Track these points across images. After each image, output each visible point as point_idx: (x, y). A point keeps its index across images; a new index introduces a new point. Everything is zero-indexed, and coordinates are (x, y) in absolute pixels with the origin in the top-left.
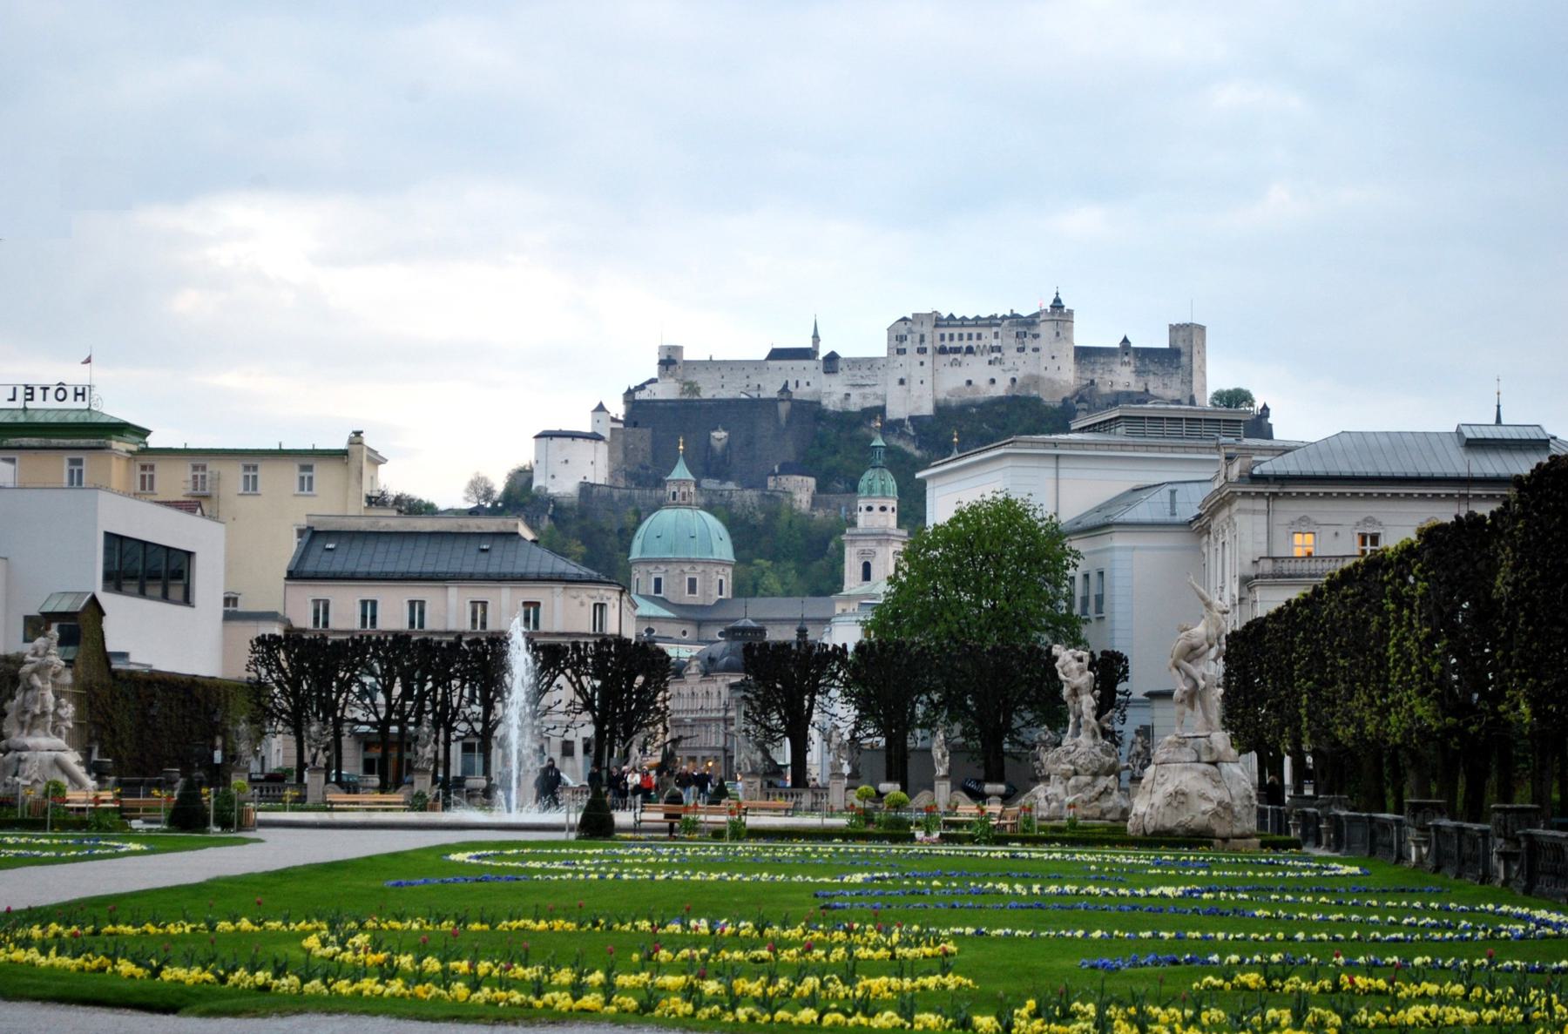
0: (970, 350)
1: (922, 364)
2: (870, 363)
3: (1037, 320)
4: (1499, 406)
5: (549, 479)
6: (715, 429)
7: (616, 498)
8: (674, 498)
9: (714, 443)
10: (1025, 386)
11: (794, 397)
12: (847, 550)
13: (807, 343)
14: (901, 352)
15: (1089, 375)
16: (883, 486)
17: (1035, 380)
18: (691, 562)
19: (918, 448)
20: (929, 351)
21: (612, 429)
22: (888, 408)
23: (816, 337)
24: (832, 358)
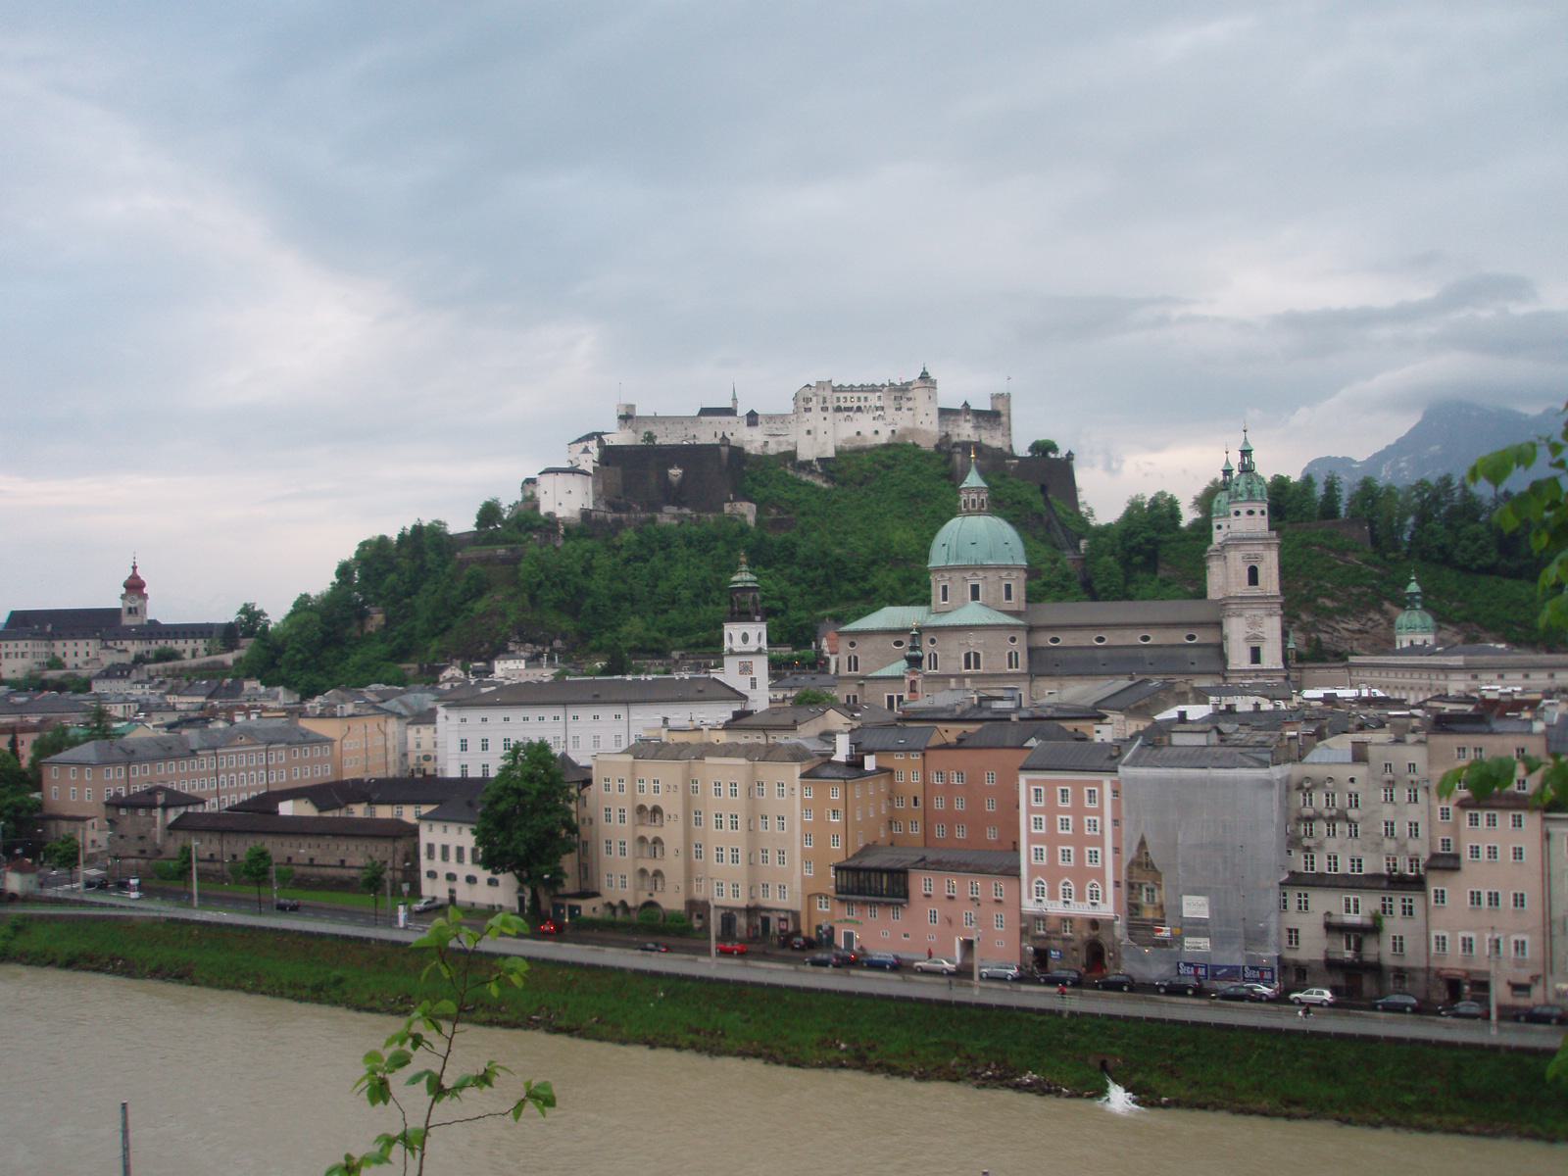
0: (859, 409)
1: (825, 419)
2: (782, 418)
3: (911, 388)
5: (557, 506)
6: (672, 467)
7: (609, 521)
8: (974, 505)
9: (670, 477)
10: (903, 436)
11: (732, 444)
15: (944, 429)
17: (912, 432)
18: (1007, 568)
19: (826, 482)
23: (735, 399)
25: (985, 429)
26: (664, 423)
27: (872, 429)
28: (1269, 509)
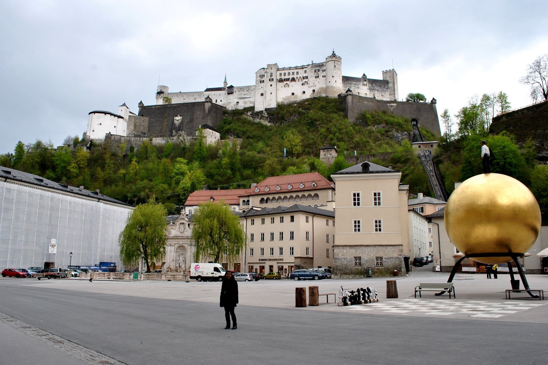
0: (293, 80)
1: (271, 85)
2: (248, 88)
6: (177, 116)
9: (175, 122)
10: (318, 93)
19: (270, 122)
20: (275, 80)
21: (129, 116)
23: (225, 82)
24: (231, 87)
26: (183, 96)
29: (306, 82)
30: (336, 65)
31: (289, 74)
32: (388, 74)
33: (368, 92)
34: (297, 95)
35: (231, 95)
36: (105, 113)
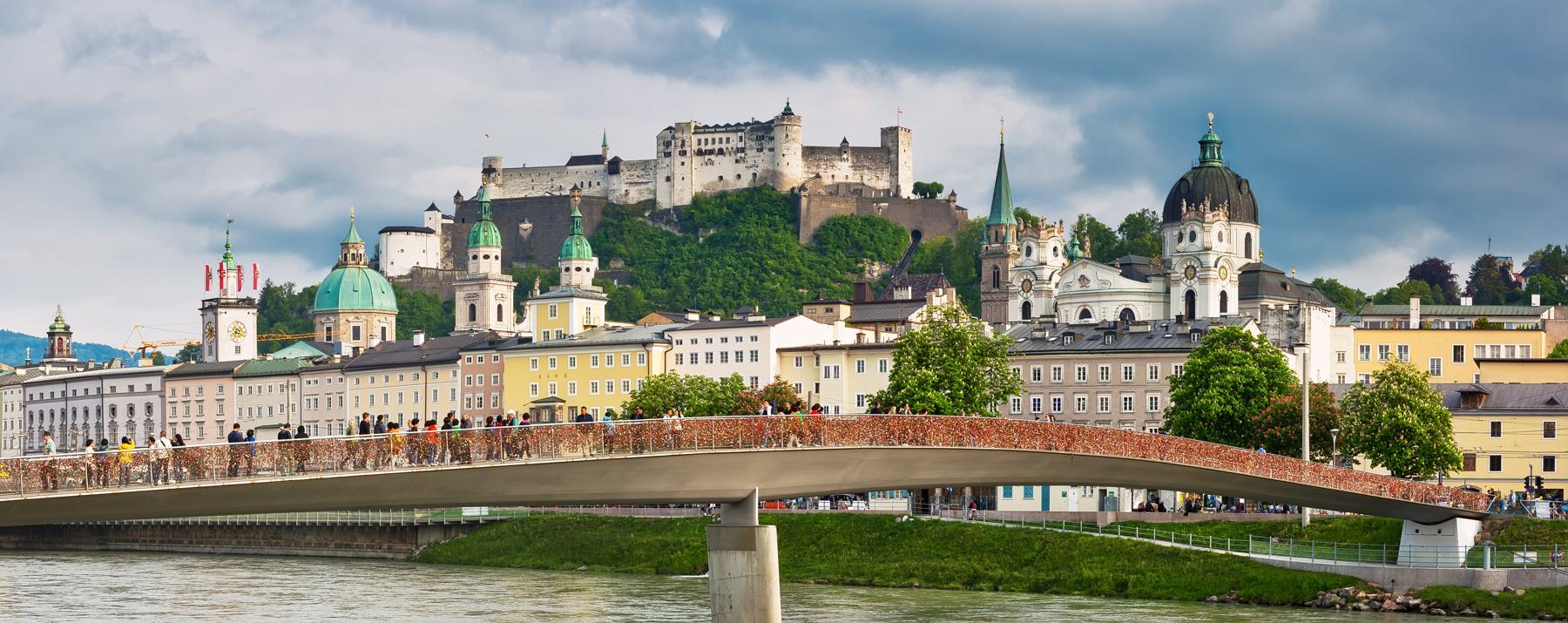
0: (721, 152)
1: (683, 164)
2: (645, 165)
3: (773, 125)
4: (1002, 145)
6: (523, 222)
9: (521, 232)
10: (761, 180)
12: (457, 293)
13: (597, 150)
14: (668, 155)
15: (815, 170)
16: (486, 237)
21: (442, 224)
22: (659, 199)
23: (604, 145)
25: (868, 168)
27: (731, 174)
28: (503, 252)
29: (741, 157)
30: (789, 134)
31: (714, 140)
32: (890, 135)
33: (850, 172)
34: (727, 181)
35: (614, 179)
36: (408, 230)
